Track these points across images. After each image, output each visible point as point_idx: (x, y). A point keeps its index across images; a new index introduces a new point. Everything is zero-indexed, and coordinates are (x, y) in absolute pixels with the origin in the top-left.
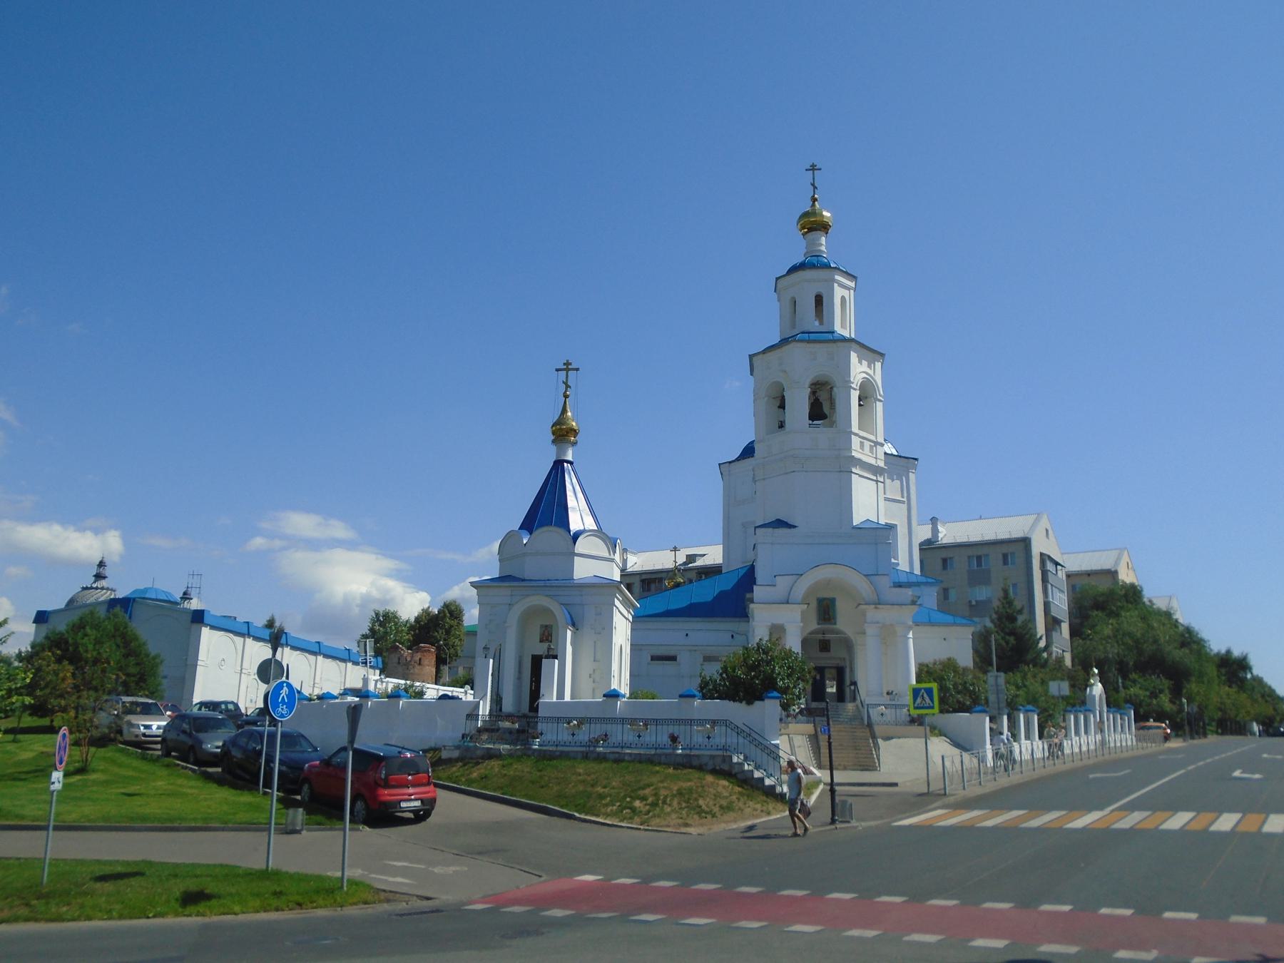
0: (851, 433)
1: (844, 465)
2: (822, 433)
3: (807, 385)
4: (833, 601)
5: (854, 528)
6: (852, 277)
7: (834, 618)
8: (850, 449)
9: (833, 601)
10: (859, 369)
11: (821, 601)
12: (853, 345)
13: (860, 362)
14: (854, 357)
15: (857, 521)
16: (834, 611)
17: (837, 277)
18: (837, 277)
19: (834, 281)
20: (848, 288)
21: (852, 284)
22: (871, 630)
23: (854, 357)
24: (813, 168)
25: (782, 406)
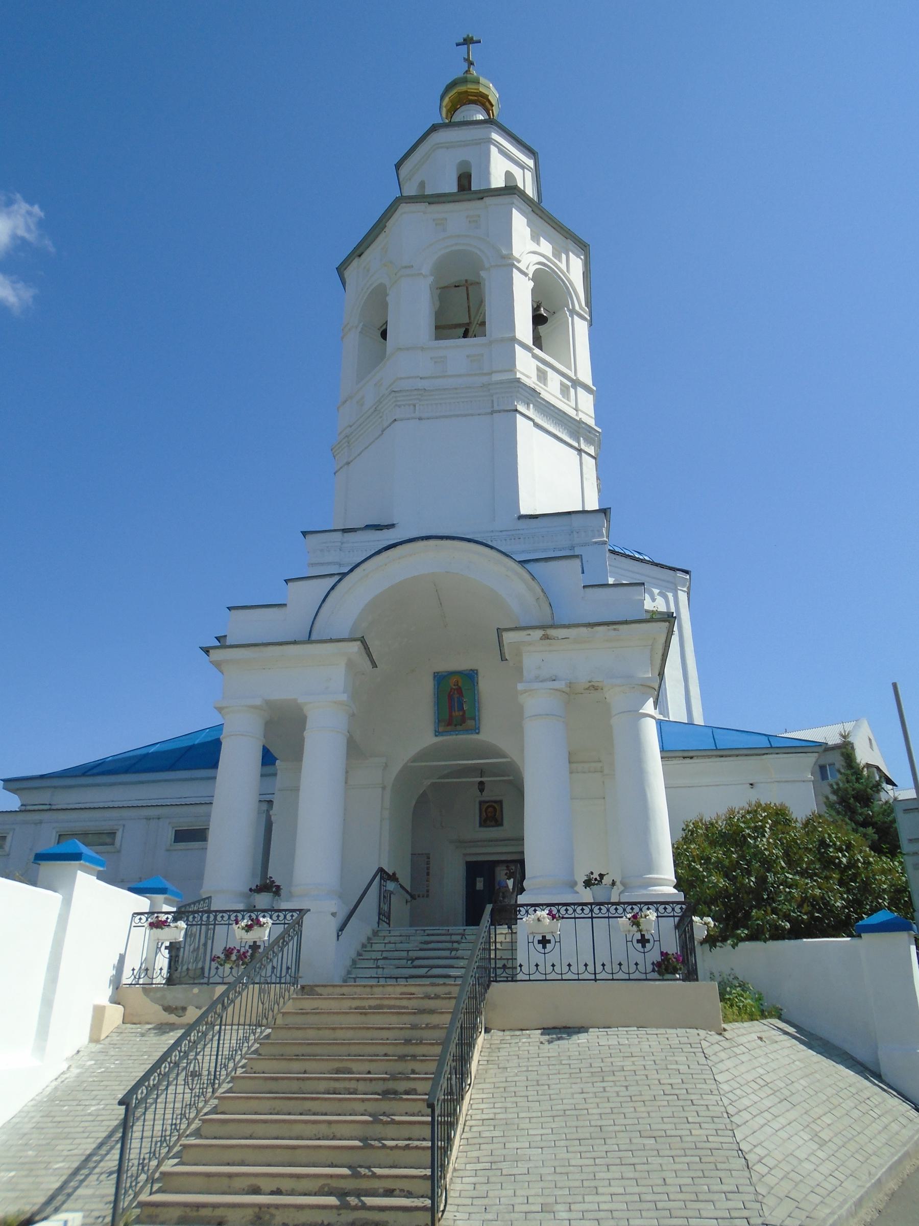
0: (514, 340)
1: (503, 399)
2: (458, 350)
3: (426, 269)
4: (471, 676)
5: (522, 517)
6: (530, 151)
8: (512, 367)
9: (471, 676)
10: (528, 246)
11: (440, 678)
12: (516, 199)
13: (535, 238)
14: (520, 223)
15: (525, 509)
16: (475, 702)
17: (495, 136)
18: (495, 136)
19: (490, 141)
20: (522, 167)
21: (531, 163)
22: (537, 702)
23: (520, 223)
24: (468, 41)
25: (384, 335)
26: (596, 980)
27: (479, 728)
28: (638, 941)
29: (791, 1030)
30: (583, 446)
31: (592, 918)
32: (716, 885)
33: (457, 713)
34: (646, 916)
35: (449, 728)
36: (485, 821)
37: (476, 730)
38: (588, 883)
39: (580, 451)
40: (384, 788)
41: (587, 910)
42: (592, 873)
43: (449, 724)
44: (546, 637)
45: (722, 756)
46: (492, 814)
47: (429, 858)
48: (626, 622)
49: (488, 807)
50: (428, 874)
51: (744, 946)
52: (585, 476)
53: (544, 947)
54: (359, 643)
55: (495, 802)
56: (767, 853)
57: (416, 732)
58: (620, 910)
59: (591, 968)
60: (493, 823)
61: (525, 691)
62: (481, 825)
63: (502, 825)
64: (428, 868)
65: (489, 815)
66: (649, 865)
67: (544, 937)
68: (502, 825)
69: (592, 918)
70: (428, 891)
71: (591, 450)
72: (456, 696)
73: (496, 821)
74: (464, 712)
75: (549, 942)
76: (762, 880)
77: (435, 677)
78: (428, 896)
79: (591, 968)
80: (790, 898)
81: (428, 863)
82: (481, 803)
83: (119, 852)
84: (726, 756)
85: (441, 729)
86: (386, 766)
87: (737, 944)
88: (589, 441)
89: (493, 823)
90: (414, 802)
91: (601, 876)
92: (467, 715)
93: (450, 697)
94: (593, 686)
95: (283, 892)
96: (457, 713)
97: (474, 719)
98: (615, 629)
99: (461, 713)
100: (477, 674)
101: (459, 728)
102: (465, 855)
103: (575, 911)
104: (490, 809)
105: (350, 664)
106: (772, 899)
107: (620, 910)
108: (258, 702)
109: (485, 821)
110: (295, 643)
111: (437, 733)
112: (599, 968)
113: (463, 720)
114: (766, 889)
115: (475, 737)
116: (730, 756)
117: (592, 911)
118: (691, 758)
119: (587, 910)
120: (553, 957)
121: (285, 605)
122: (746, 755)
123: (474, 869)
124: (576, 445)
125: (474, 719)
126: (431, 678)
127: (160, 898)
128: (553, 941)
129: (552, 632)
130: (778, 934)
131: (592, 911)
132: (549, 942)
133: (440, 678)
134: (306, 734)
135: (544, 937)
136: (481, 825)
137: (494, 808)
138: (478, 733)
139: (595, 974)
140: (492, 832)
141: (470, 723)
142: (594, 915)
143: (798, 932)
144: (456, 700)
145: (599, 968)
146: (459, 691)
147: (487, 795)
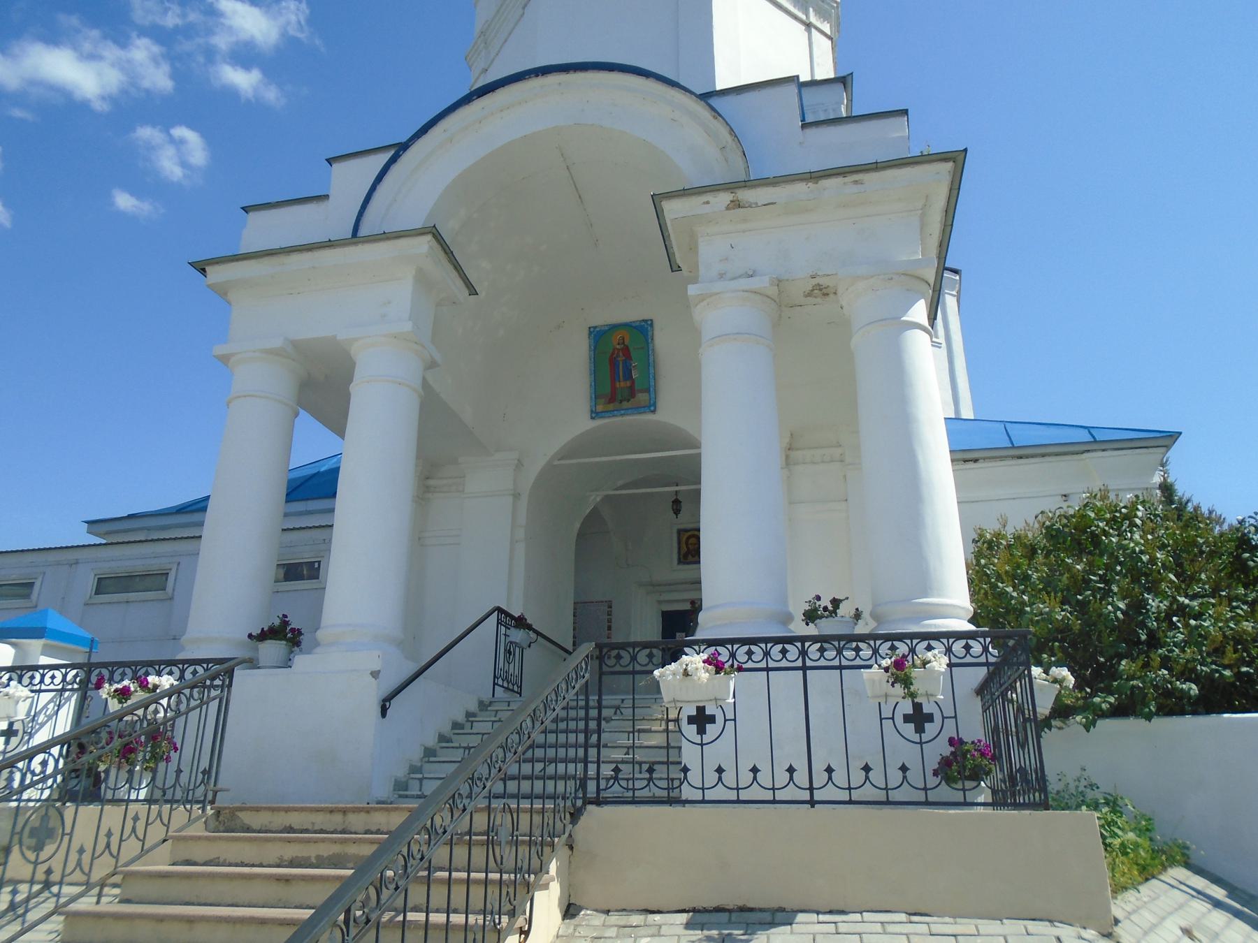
4: (643, 329)
7: (650, 389)
9: (643, 329)
11: (598, 336)
16: (649, 363)
26: (812, 803)
27: (655, 405)
28: (907, 719)
29: (1219, 893)
30: (813, 19)
31: (804, 668)
32: (1048, 618)
33: (622, 384)
34: (925, 663)
35: (611, 407)
36: (685, 556)
37: (652, 407)
38: (811, 616)
39: (808, 26)
40: (516, 496)
41: (793, 651)
42: (818, 598)
43: (612, 399)
44: (736, 204)
45: (1020, 457)
48: (876, 167)
49: (688, 538)
50: (609, 628)
51: (1104, 725)
52: (815, 60)
53: (701, 731)
54: (429, 237)
56: (1145, 558)
57: (562, 411)
58: (866, 652)
59: (801, 777)
61: (702, 298)
62: (680, 562)
64: (609, 621)
66: (924, 581)
67: (701, 710)
69: (804, 668)
71: (826, 28)
72: (621, 358)
75: (712, 719)
76: (1138, 606)
77: (590, 333)
79: (801, 777)
80: (1196, 637)
82: (680, 532)
83: (171, 599)
84: (1027, 457)
85: (600, 408)
86: (519, 465)
87: (1094, 723)
88: (823, 15)
90: (578, 525)
91: (836, 603)
92: (637, 387)
93: (613, 363)
94: (819, 287)
95: (305, 639)
96: (622, 384)
97: (648, 391)
98: (856, 182)
99: (628, 383)
100: (652, 325)
101: (625, 404)
102: (660, 602)
103: (767, 654)
105: (423, 281)
106: (1154, 641)
107: (866, 652)
108: (277, 343)
109: (685, 556)
110: (330, 244)
111: (595, 414)
112: (820, 778)
113: (632, 392)
114: (1143, 625)
115: (650, 417)
116: (1033, 456)
117: (803, 653)
118: (976, 461)
119: (793, 651)
120: (720, 752)
121: (326, 197)
122: (1057, 454)
124: (804, 17)
125: (648, 391)
126: (586, 333)
127: (35, 645)
128: (720, 719)
129: (746, 195)
130: (1173, 705)
131: (803, 653)
132: (712, 719)
133: (598, 336)
134: (354, 389)
135: (701, 710)
136: (680, 562)
138: (654, 412)
139: (811, 789)
141: (642, 397)
142: (809, 663)
143: (1217, 698)
144: (623, 366)
145: (820, 778)
146: (626, 351)
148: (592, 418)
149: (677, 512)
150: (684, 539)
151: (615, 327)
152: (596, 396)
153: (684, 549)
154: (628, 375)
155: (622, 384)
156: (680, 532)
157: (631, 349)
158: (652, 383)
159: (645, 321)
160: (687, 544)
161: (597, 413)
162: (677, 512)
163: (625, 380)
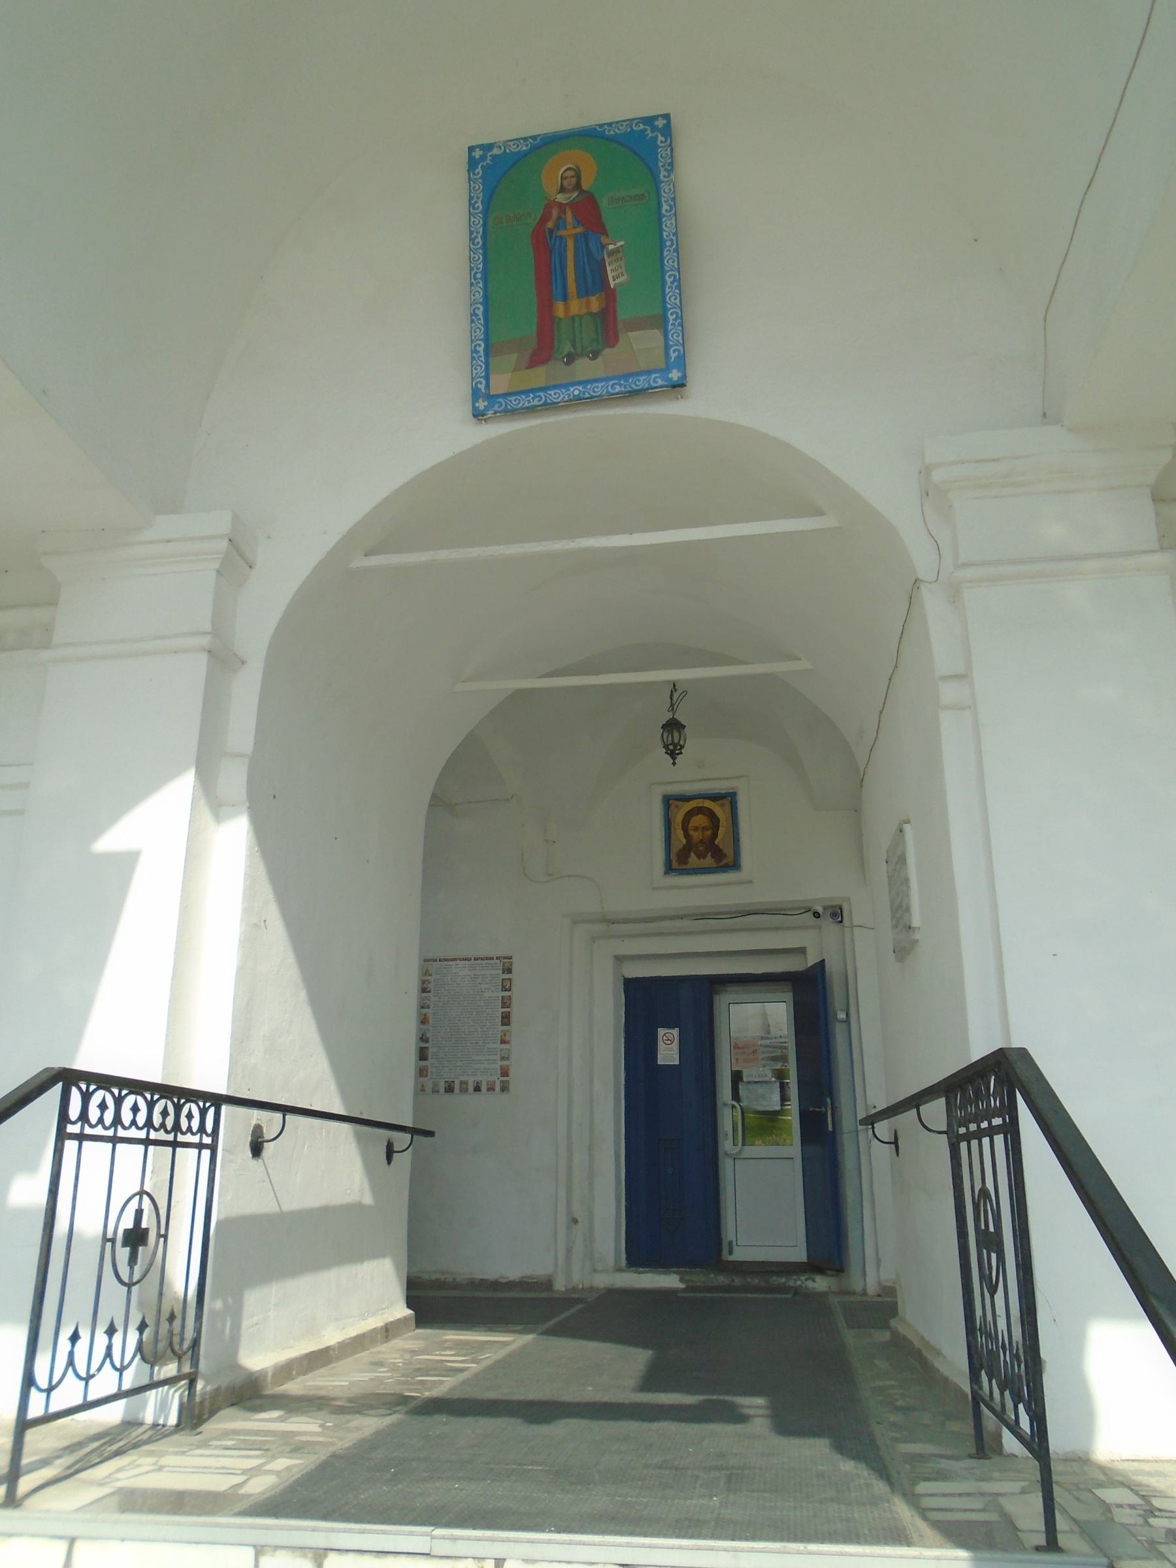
4: (640, 150)
16: (660, 247)
33: (574, 307)
40: (222, 660)
43: (541, 354)
46: (702, 836)
47: (509, 971)
49: (690, 814)
50: (506, 1019)
55: (716, 797)
60: (709, 861)
62: (669, 869)
63: (735, 865)
64: (506, 1003)
65: (696, 836)
68: (735, 865)
70: (505, 1073)
72: (571, 229)
73: (718, 854)
74: (610, 296)
77: (472, 163)
78: (505, 1088)
81: (506, 986)
82: (669, 801)
85: (500, 383)
86: (236, 560)
89: (709, 861)
92: (622, 315)
93: (544, 244)
96: (574, 307)
97: (659, 322)
99: (595, 304)
100: (667, 131)
101: (584, 368)
102: (619, 959)
104: (699, 820)
111: (485, 404)
113: (607, 328)
123: (650, 1004)
125: (659, 322)
136: (669, 869)
137: (711, 815)
140: (705, 890)
141: (641, 345)
146: (588, 211)
147: (695, 773)
148: (478, 415)
149: (673, 751)
150: (679, 818)
151: (548, 144)
152: (489, 348)
153: (680, 839)
154: (594, 279)
155: (576, 307)
156: (669, 801)
157: (603, 203)
158: (671, 300)
159: (649, 121)
160: (685, 829)
161: (490, 398)
162: (673, 751)
163: (584, 291)
